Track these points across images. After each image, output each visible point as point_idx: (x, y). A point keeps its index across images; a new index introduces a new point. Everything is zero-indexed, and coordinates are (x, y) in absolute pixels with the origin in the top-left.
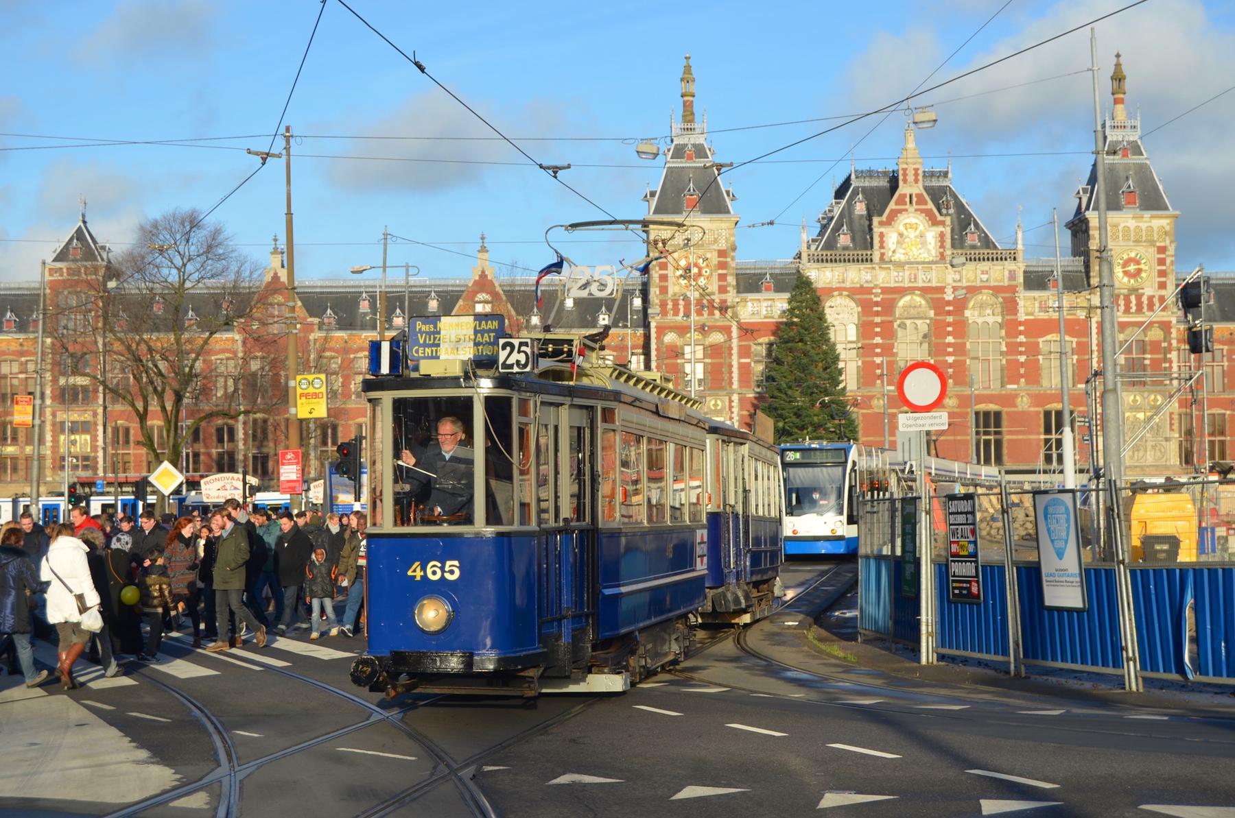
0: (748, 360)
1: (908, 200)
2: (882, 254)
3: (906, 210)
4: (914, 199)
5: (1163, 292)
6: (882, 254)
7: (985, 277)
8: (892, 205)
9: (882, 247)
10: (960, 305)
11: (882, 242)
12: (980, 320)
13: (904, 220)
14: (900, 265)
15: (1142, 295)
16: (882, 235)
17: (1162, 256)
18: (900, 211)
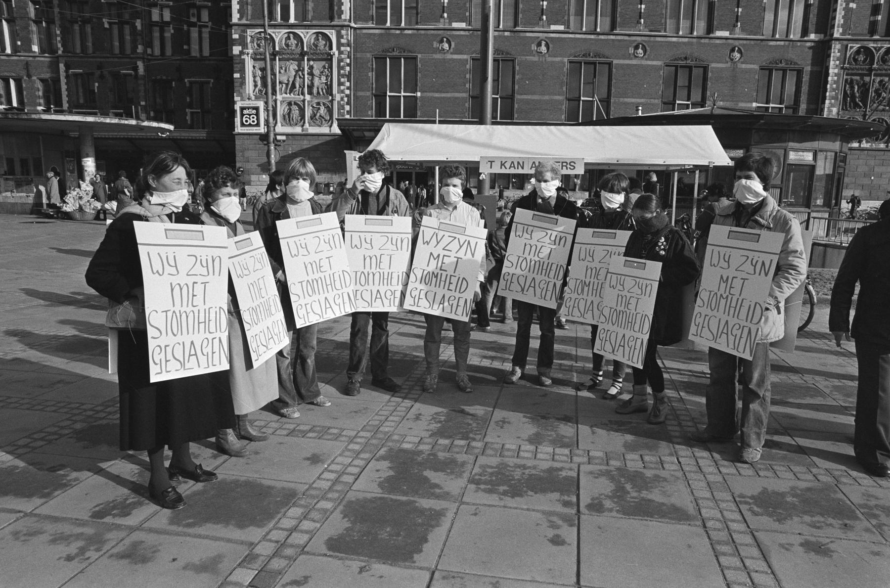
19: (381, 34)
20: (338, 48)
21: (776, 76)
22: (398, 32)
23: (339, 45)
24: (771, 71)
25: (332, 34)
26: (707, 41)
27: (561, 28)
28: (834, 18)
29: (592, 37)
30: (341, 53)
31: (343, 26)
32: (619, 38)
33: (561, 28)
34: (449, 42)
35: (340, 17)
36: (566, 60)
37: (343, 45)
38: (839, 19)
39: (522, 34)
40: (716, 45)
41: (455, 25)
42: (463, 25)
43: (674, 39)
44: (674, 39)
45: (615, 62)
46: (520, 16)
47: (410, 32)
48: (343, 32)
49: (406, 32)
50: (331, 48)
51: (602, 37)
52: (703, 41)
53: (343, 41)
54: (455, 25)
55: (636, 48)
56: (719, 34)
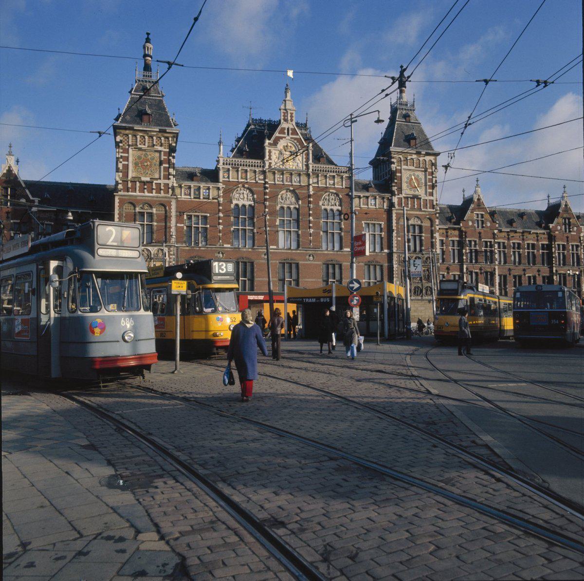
0: (182, 225)
1: (286, 131)
2: (270, 163)
3: (285, 137)
4: (290, 132)
5: (431, 198)
6: (270, 163)
7: (332, 182)
8: (277, 134)
9: (270, 159)
10: (318, 197)
11: (270, 156)
12: (329, 208)
13: (281, 144)
14: (282, 172)
15: (420, 199)
16: (270, 152)
17: (431, 177)
18: (282, 138)
19: (189, 250)
20: (169, 256)
21: (372, 268)
22: (198, 249)
23: (169, 255)
24: (369, 266)
25: (166, 250)
26: (340, 253)
27: (275, 247)
28: (393, 244)
29: (290, 251)
30: (170, 258)
31: (171, 246)
32: (301, 251)
33: (275, 247)
34: (223, 254)
35: (170, 242)
36: (278, 262)
37: (171, 255)
38: (395, 245)
39: (257, 250)
40: (344, 255)
41: (225, 246)
42: (229, 246)
43: (326, 252)
44: (326, 252)
45: (300, 262)
46: (256, 242)
47: (203, 249)
48: (172, 249)
49: (202, 249)
50: (165, 256)
51: (294, 251)
52: (338, 253)
53: (172, 253)
54: (225, 246)
55: (310, 256)
56: (345, 249)
